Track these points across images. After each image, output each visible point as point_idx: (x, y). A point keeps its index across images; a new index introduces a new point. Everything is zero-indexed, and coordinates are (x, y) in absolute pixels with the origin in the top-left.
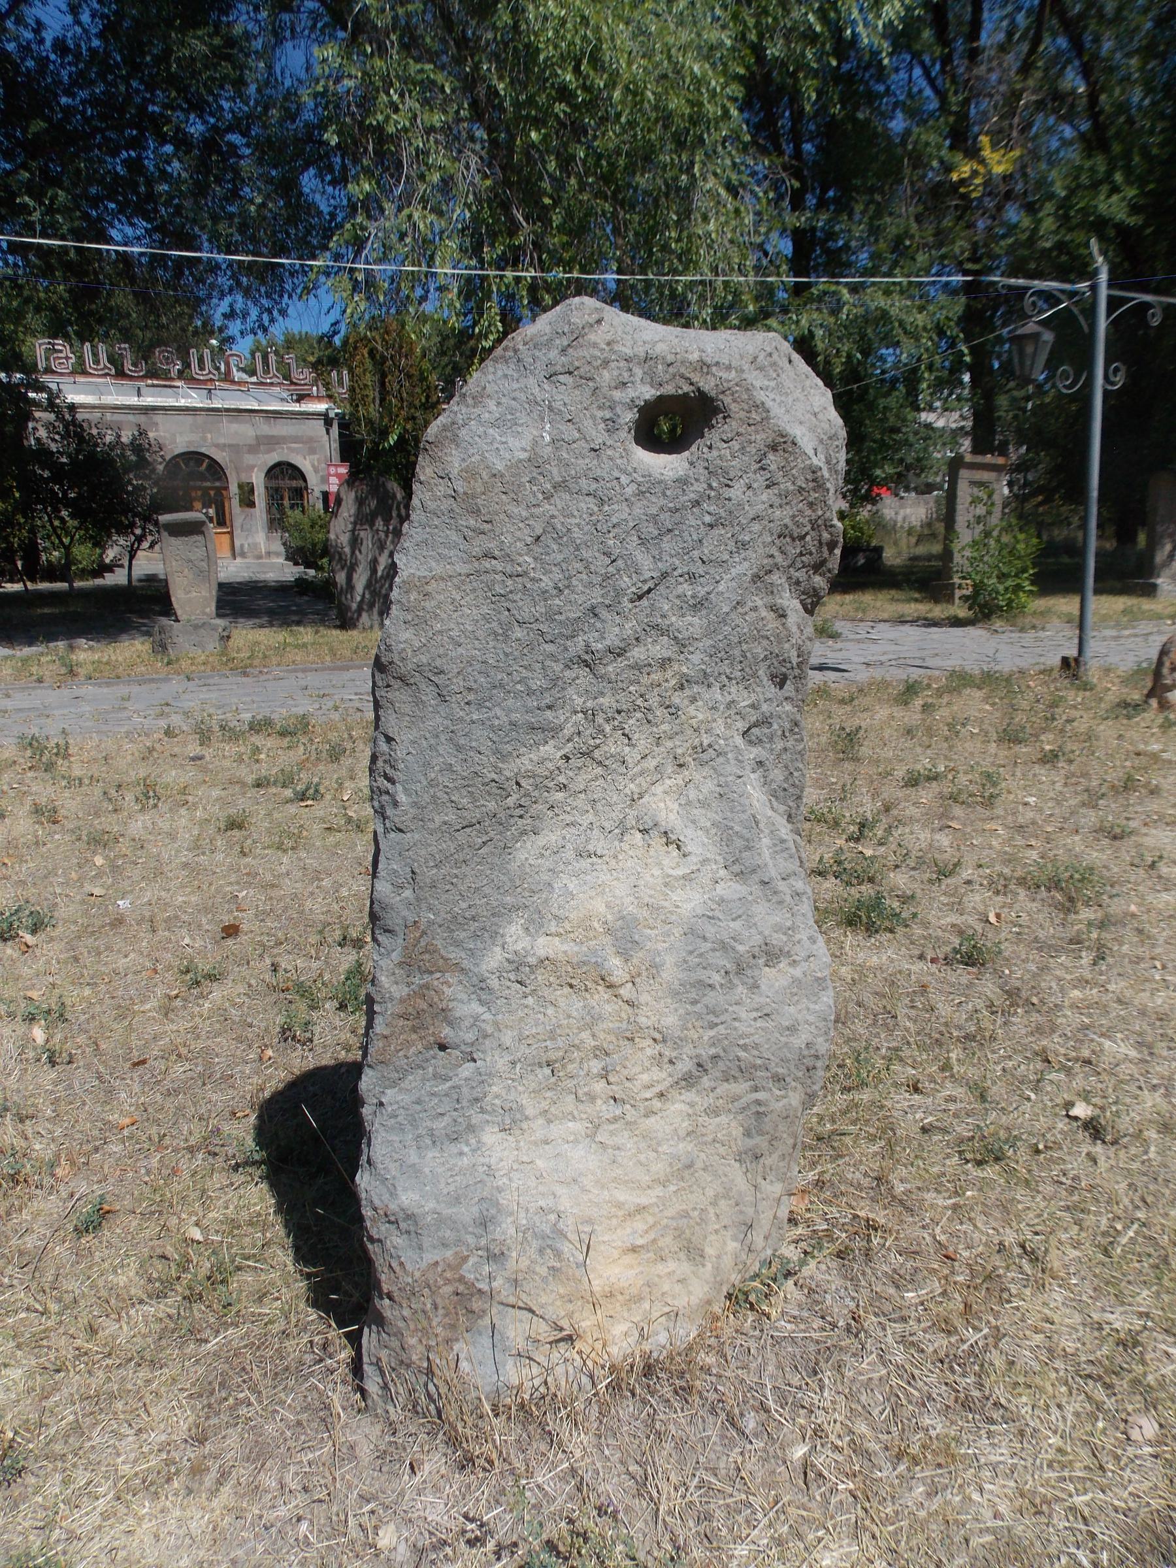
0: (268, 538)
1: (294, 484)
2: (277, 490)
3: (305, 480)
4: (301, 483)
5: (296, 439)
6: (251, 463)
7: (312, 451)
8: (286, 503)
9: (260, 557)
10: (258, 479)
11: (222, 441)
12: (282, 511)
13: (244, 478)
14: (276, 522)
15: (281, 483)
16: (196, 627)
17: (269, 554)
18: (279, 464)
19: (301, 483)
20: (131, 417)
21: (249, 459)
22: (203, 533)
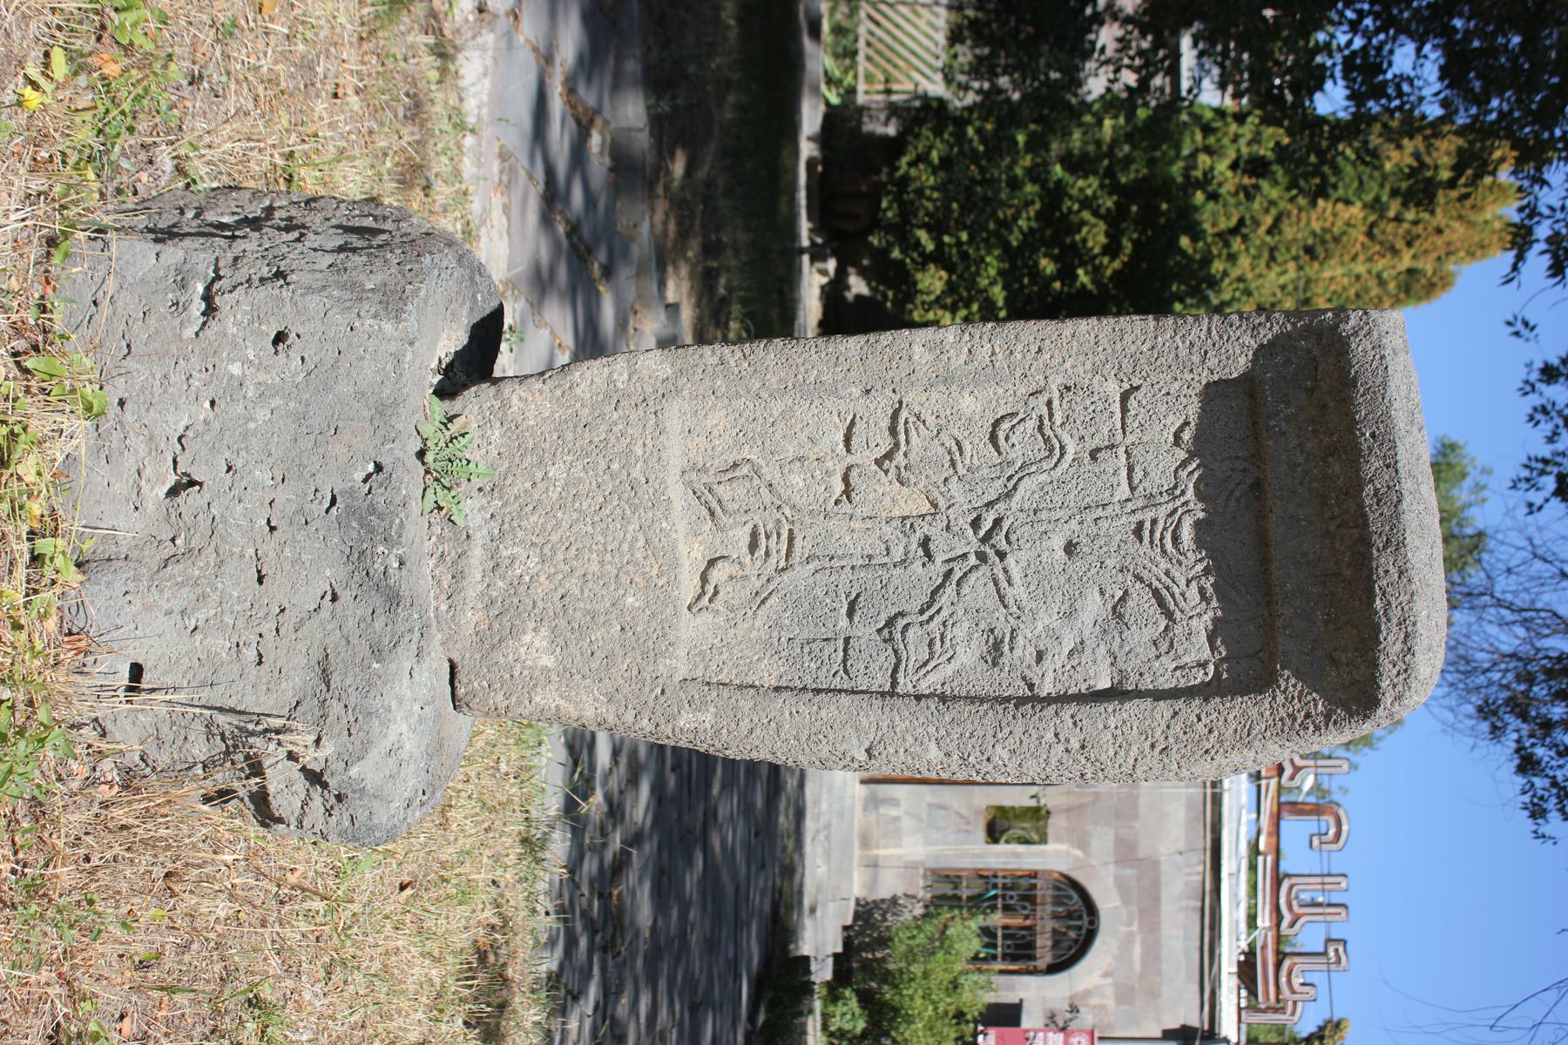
0: (911, 866)
1: (1043, 942)
2: (1029, 898)
3: (1053, 969)
4: (1045, 957)
5: (1153, 955)
6: (1095, 844)
7: (1124, 995)
8: (997, 919)
9: (865, 843)
10: (1051, 856)
12: (977, 903)
13: (1055, 824)
14: (951, 893)
15: (1045, 910)
16: (362, 519)
17: (873, 865)
18: (1090, 908)
19: (1045, 957)
21: (1103, 840)
22: (1245, 669)
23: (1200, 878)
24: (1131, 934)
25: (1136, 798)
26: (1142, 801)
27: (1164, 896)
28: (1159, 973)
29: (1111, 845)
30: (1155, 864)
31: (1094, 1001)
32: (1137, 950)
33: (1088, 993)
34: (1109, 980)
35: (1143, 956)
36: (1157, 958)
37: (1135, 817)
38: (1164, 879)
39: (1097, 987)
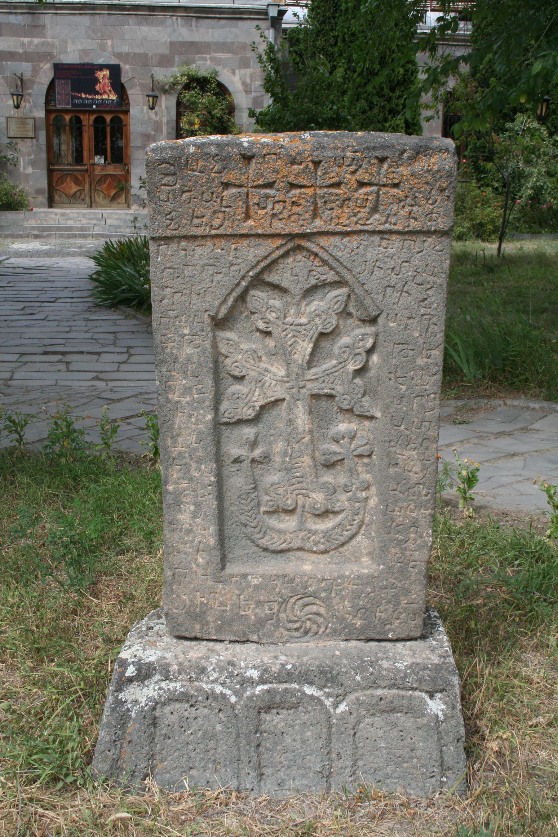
5: (223, 47)
11: (126, 49)
20: (12, 19)
23: (179, 19)
24: (211, 59)
25: (135, 54)
26: (137, 51)
27: (190, 39)
28: (233, 43)
29: (162, 69)
30: (172, 44)
31: (248, 81)
32: (220, 55)
33: (244, 84)
34: (237, 72)
35: (223, 52)
36: (224, 44)
37: (146, 55)
38: (181, 39)
39: (241, 79)
